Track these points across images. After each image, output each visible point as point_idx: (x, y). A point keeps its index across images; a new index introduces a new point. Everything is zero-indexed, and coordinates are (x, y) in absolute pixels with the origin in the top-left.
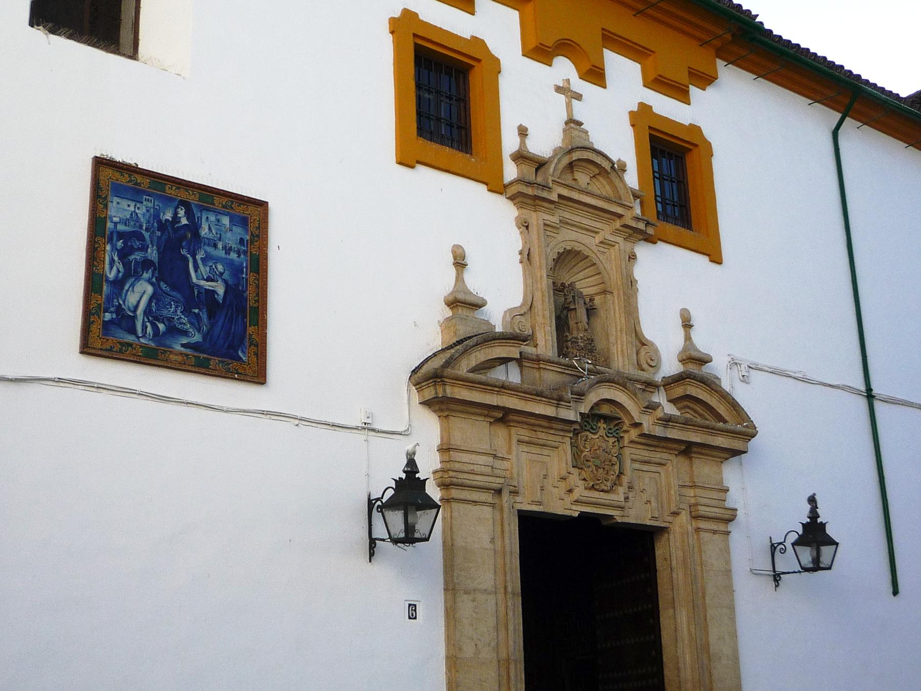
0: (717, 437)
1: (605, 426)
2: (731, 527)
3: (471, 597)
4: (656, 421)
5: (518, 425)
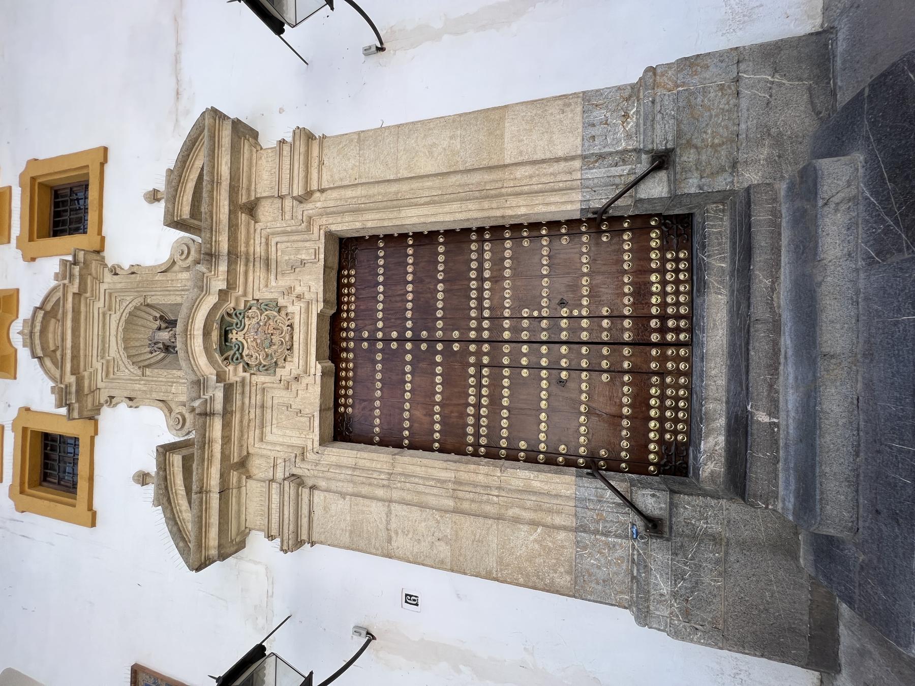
0: (223, 173)
1: (234, 332)
2: (318, 134)
3: (393, 535)
4: (213, 273)
5: (245, 445)
